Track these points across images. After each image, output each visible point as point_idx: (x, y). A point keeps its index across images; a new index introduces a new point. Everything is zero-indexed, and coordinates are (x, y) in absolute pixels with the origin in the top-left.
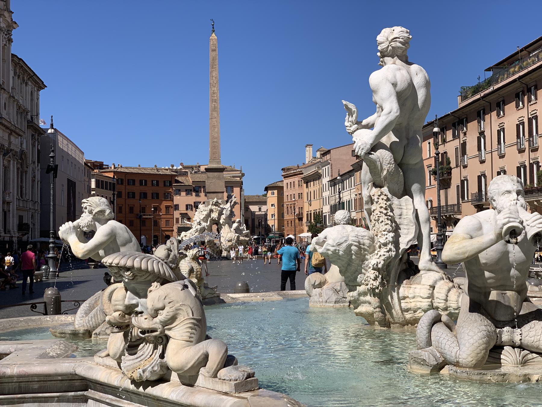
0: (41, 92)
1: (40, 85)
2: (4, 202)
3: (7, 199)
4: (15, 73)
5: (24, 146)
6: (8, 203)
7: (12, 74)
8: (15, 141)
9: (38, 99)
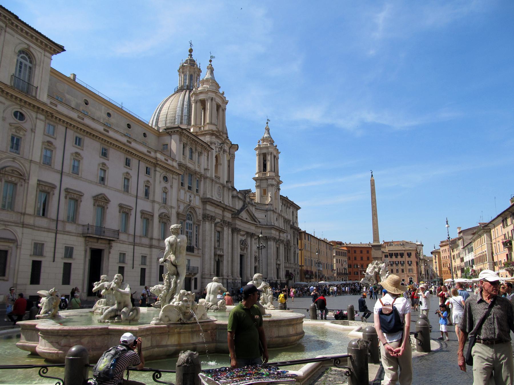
0: (299, 211)
1: (298, 208)
2: (276, 264)
3: (278, 262)
4: (283, 204)
5: (289, 237)
6: (279, 265)
7: (281, 204)
8: (283, 236)
9: (297, 214)
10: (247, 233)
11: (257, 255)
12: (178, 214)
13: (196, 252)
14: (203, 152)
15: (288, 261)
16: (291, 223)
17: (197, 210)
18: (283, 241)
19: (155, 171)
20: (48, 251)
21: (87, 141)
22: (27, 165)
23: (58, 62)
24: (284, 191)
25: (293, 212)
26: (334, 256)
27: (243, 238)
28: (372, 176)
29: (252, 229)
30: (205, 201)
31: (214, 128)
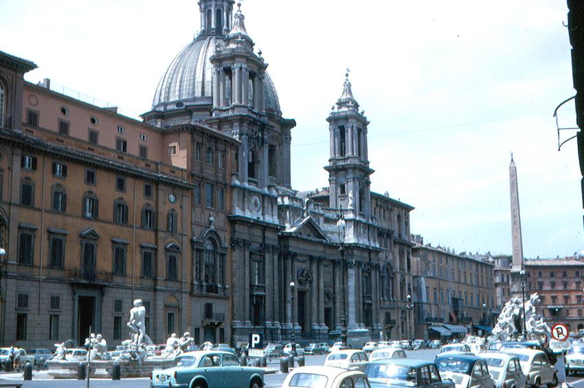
0: (411, 213)
4: (377, 205)
5: (390, 257)
6: (370, 305)
10: (311, 258)
11: (331, 290)
12: (192, 242)
13: (221, 293)
14: (228, 149)
15: (389, 298)
16: (396, 235)
17: (221, 234)
18: (377, 267)
19: (157, 190)
20: (32, 304)
21: (71, 168)
22: (6, 208)
23: (30, 77)
24: (378, 185)
25: (399, 216)
26: (496, 285)
27: (305, 266)
28: (512, 160)
29: (318, 251)
30: (234, 221)
31: (244, 112)
